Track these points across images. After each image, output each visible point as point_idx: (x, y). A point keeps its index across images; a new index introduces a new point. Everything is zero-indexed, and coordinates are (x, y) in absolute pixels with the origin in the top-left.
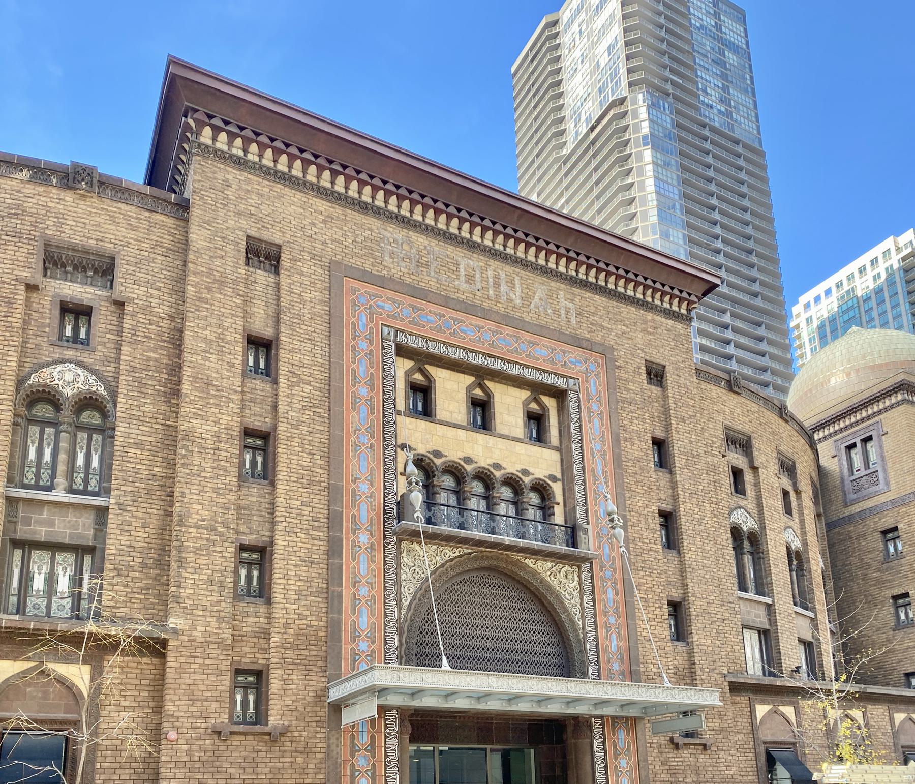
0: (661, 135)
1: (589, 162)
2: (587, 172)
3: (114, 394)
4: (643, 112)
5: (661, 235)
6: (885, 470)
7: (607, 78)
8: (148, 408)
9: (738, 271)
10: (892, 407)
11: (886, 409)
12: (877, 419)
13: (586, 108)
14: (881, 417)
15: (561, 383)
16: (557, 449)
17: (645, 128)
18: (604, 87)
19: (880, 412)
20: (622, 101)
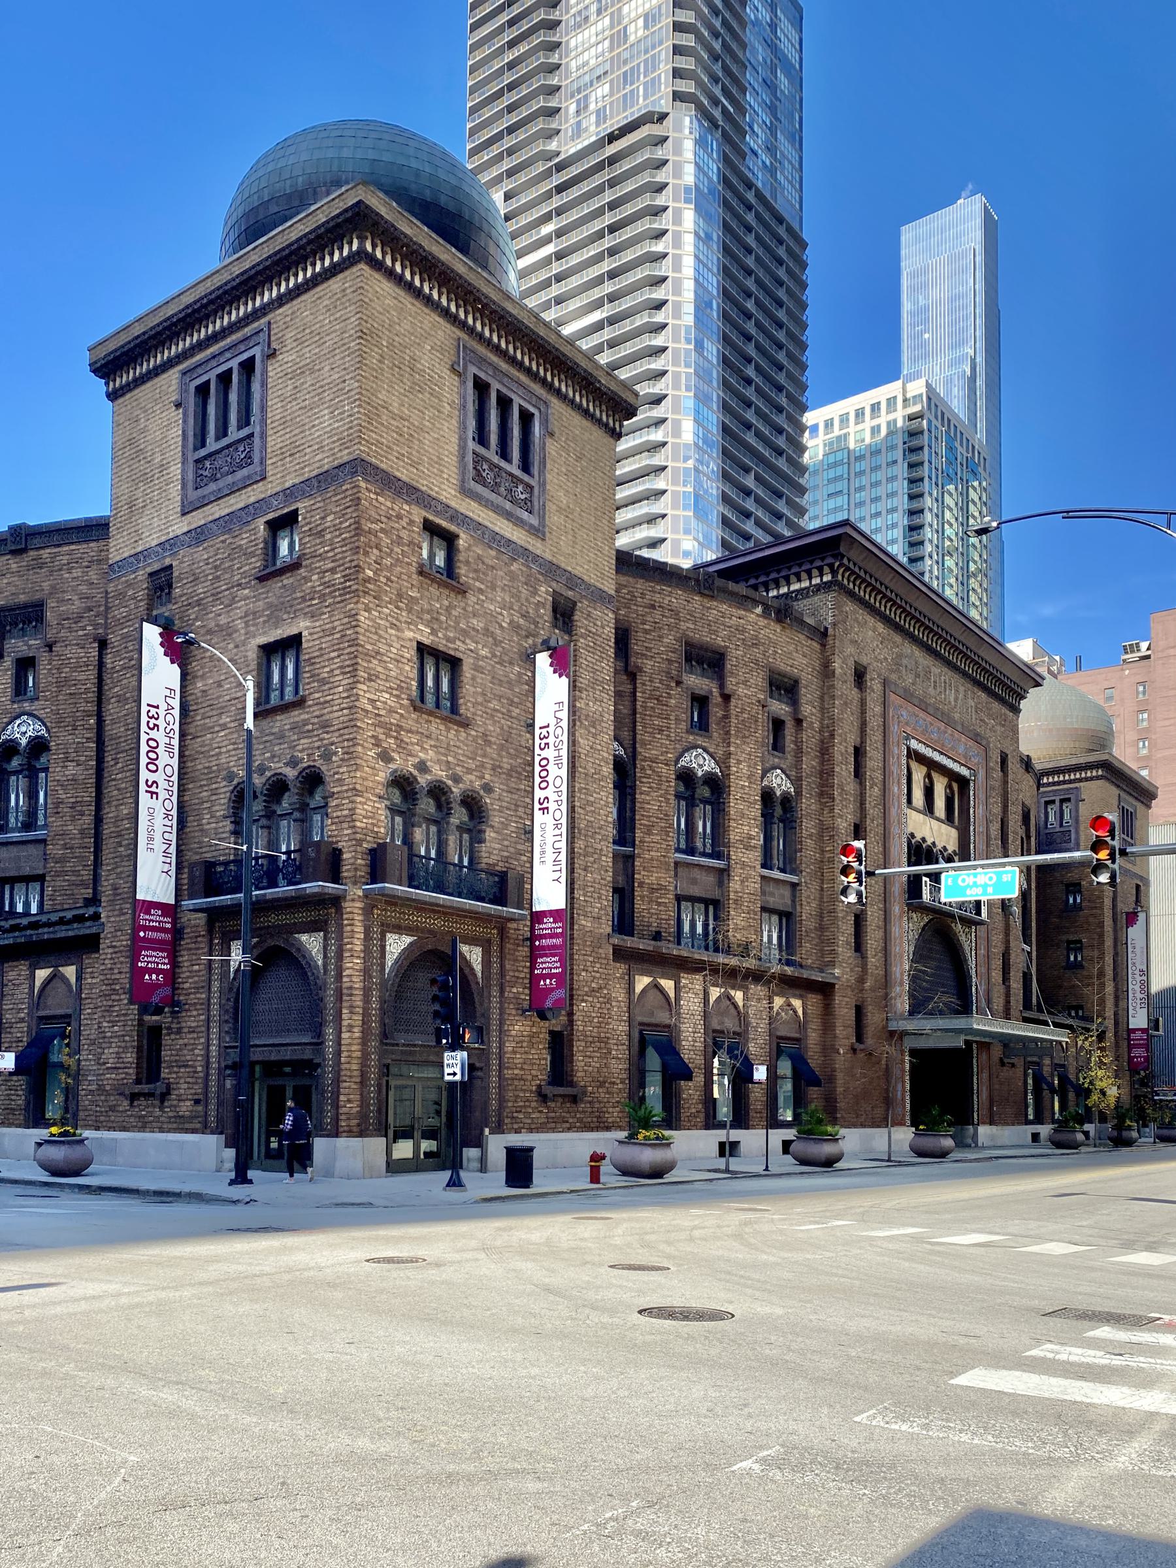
0: (706, 191)
1: (600, 190)
2: (595, 204)
3: (799, 793)
4: (689, 145)
5: (696, 346)
6: (1077, 833)
7: (638, 65)
8: (813, 807)
9: (766, 414)
10: (1092, 779)
11: (1087, 779)
12: (1077, 785)
13: (599, 92)
14: (1082, 784)
15: (964, 772)
16: (957, 828)
17: (689, 176)
18: (632, 75)
19: (1080, 780)
20: (663, 117)
